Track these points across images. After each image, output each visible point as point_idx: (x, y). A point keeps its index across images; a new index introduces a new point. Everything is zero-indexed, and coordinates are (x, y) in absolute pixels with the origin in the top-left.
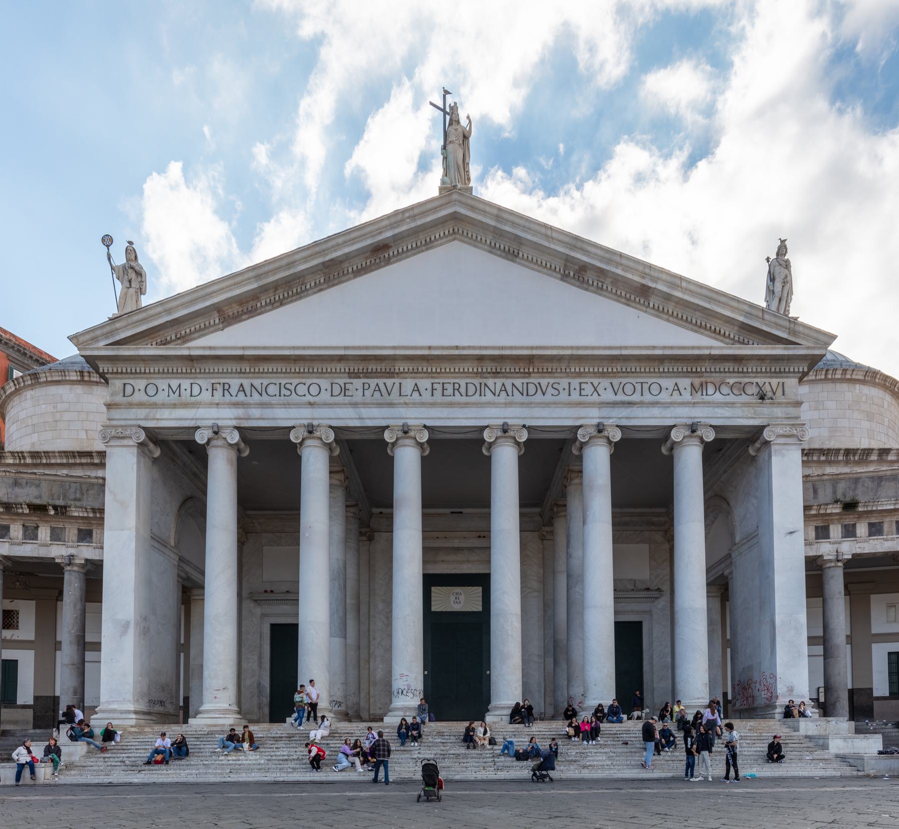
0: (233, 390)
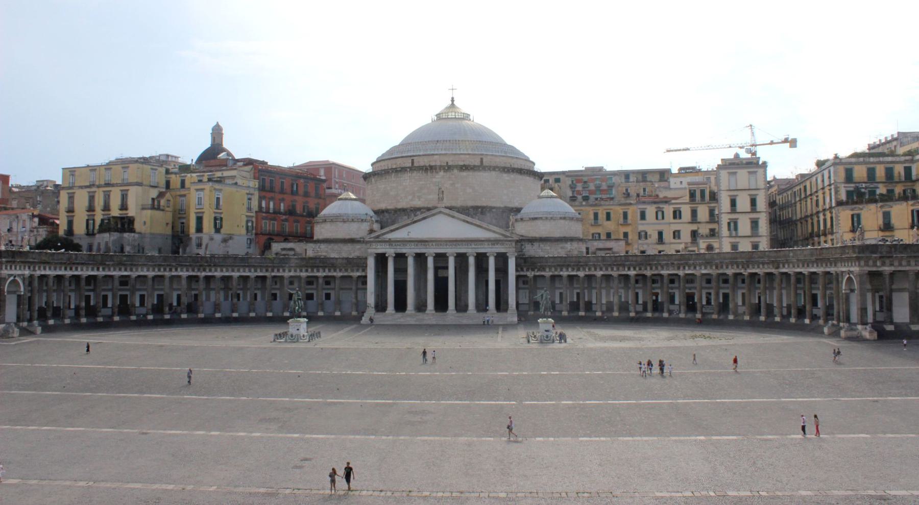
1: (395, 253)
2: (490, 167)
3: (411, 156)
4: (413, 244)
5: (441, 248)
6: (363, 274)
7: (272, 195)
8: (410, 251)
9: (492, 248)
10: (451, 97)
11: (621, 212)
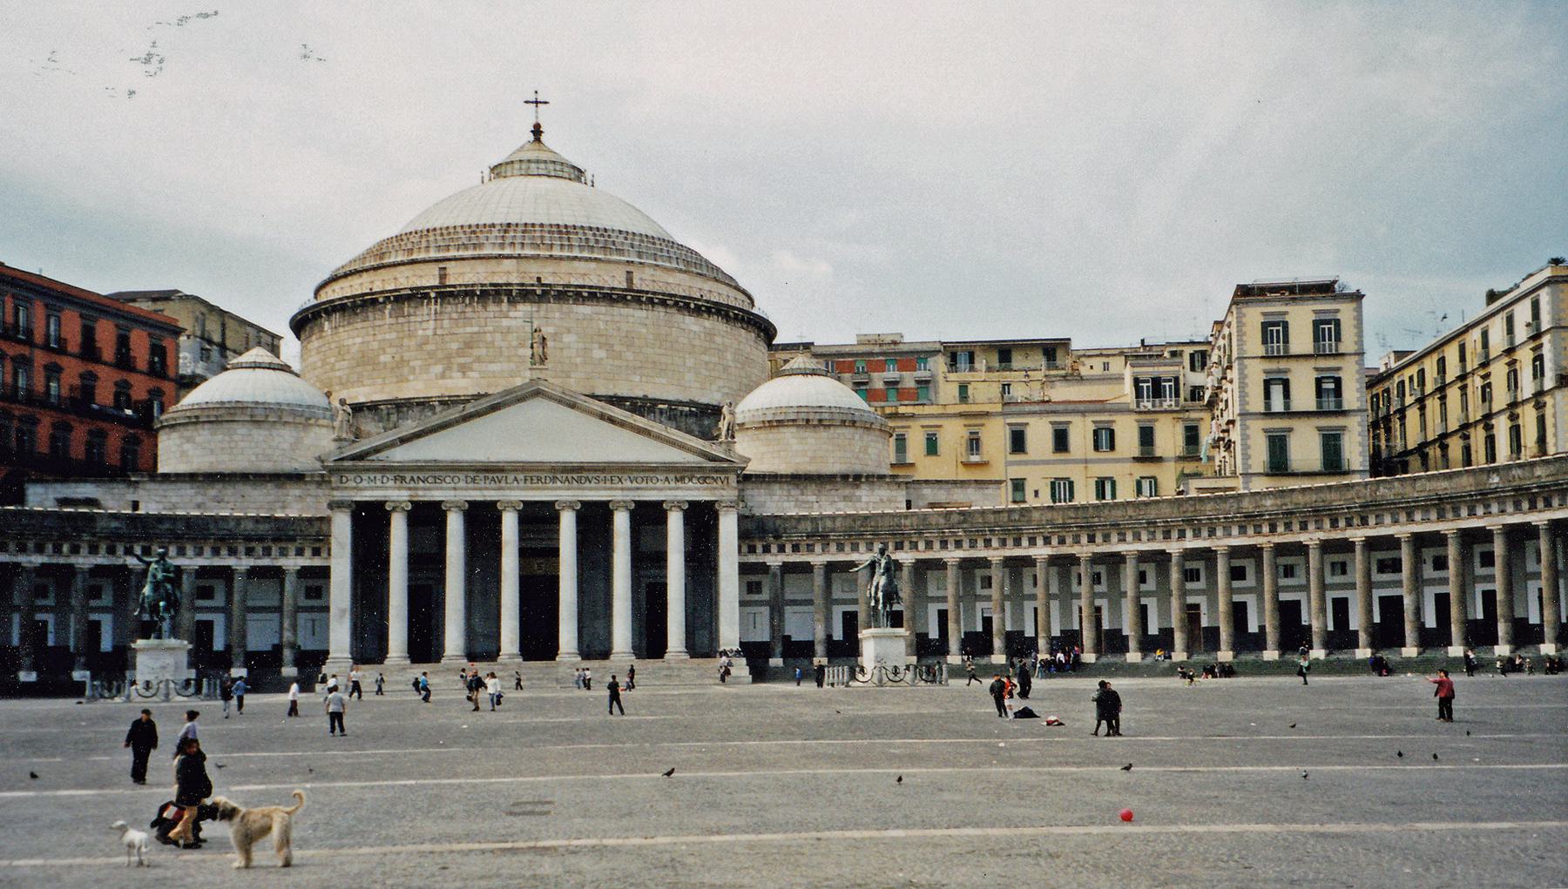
0: (408, 480)
1: (412, 502)
2: (654, 293)
3: (437, 261)
4: (462, 476)
5: (539, 489)
6: (317, 562)
7: (25, 351)
8: (453, 494)
9: (678, 488)
10: (533, 122)
11: (965, 433)
